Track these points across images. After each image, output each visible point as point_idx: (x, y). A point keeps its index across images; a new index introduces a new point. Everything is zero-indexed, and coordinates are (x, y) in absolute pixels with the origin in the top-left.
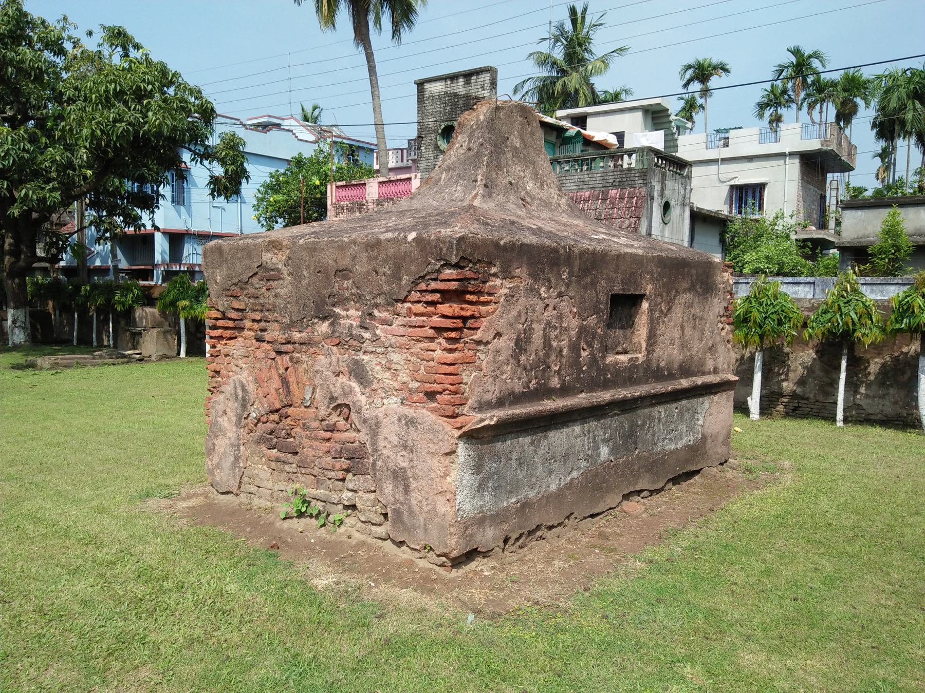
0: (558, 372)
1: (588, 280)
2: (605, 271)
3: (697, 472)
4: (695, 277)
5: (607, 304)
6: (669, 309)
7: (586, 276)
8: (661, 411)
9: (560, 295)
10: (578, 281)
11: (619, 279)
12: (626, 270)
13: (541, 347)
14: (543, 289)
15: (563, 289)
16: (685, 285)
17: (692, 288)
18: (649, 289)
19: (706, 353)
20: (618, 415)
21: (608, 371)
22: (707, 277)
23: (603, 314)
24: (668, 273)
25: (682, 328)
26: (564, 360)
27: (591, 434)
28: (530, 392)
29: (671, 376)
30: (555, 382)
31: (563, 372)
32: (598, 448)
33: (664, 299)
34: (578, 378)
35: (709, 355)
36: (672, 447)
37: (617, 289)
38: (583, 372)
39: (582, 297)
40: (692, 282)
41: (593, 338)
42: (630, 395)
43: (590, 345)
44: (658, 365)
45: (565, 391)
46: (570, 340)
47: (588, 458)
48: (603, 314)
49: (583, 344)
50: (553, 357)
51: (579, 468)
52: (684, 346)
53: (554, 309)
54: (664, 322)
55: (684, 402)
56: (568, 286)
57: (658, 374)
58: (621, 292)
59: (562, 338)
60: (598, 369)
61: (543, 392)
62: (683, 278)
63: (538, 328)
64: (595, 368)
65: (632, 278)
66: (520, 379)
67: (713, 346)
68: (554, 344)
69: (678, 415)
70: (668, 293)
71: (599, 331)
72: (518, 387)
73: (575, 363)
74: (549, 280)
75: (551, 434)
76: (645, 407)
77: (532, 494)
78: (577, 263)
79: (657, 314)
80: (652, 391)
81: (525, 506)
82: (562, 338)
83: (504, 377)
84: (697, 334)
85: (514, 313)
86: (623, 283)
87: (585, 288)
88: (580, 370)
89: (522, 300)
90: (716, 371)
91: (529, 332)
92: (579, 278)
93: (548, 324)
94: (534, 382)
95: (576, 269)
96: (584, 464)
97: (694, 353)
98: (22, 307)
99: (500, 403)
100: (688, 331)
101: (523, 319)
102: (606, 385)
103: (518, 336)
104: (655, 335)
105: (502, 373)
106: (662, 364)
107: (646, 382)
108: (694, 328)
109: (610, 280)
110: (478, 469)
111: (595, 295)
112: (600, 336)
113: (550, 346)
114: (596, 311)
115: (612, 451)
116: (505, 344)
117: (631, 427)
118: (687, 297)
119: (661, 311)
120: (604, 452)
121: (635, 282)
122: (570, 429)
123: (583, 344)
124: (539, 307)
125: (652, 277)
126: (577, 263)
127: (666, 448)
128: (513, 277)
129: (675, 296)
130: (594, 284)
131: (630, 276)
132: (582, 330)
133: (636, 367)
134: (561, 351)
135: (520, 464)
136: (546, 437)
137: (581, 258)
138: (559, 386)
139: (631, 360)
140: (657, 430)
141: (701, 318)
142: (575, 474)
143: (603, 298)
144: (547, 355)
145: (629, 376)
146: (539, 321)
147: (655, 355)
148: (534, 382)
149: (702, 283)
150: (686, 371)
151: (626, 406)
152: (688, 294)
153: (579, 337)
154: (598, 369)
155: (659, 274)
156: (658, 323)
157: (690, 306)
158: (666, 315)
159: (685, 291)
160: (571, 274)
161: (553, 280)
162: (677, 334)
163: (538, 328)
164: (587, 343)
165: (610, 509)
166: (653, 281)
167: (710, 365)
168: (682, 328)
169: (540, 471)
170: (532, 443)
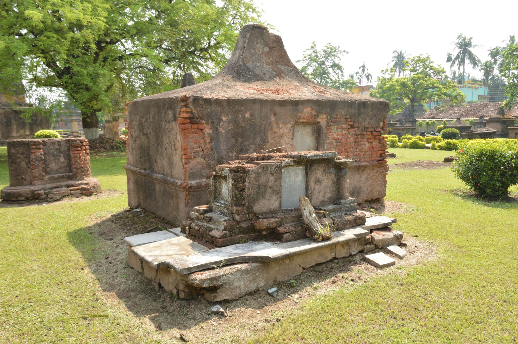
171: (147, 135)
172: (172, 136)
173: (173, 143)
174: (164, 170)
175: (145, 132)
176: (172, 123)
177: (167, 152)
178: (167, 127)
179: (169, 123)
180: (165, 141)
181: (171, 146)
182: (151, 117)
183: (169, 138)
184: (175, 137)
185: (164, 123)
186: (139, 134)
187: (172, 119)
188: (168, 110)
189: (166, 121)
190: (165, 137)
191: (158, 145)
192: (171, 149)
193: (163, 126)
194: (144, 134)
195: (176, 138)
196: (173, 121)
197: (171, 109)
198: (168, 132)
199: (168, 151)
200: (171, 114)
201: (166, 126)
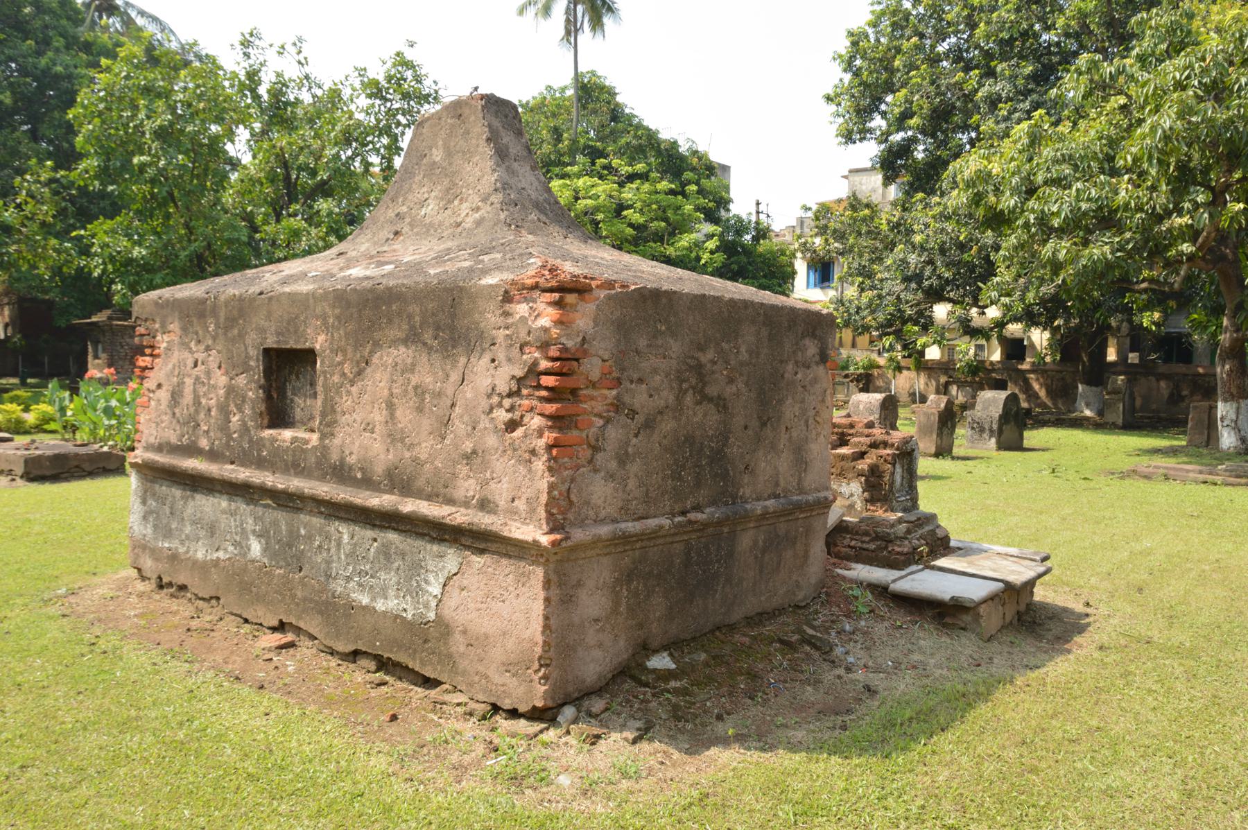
0: (207, 432)
1: (236, 331)
2: (254, 320)
3: (429, 683)
4: (417, 318)
5: (258, 360)
6: (359, 373)
7: (232, 327)
8: (344, 531)
9: (208, 349)
10: (225, 334)
11: (273, 329)
12: (281, 316)
13: (191, 403)
14: (193, 343)
15: (210, 342)
16: (395, 333)
17: (413, 337)
18: (319, 342)
19: (455, 463)
20: (274, 508)
21: (264, 446)
22: (453, 316)
23: (254, 374)
24: (355, 315)
25: (391, 407)
26: (213, 421)
27: (238, 517)
28: (182, 445)
29: (368, 483)
30: (204, 443)
31: (212, 434)
32: (248, 539)
33: (350, 355)
34: (227, 444)
35: (463, 470)
36: (365, 600)
37: (271, 342)
38: (234, 440)
39: (228, 350)
40: (412, 328)
41: (244, 401)
42: (270, 484)
43: (240, 410)
44: (342, 460)
45: (213, 455)
46: (218, 400)
47: (236, 544)
48: (254, 374)
49: (233, 408)
50: (202, 416)
51: (226, 550)
52: (395, 437)
53: (203, 364)
54: (349, 393)
55: (392, 536)
56: (214, 338)
57: (341, 473)
58: (275, 346)
59: (211, 396)
60: (251, 441)
61: (191, 450)
62: (390, 321)
63: (189, 382)
64: (246, 438)
65: (292, 324)
66: (175, 431)
67: (474, 452)
68: (204, 401)
69: (378, 551)
70: (358, 345)
71: (250, 393)
72: (174, 440)
73: (224, 427)
74: (197, 333)
75: (198, 497)
76: (311, 512)
77: (182, 550)
78: (222, 315)
79: (336, 379)
80: (306, 491)
81: (174, 557)
82: (211, 396)
83: (163, 425)
84: (426, 423)
85: (170, 366)
86: (278, 334)
87: (233, 340)
88: (229, 437)
89: (176, 353)
90: (485, 505)
91: (181, 384)
92: (227, 329)
93: (197, 379)
94: (186, 437)
95: (222, 320)
96: (231, 548)
97: (423, 457)
98: (1233, 399)
99: (159, 448)
100: (405, 415)
101: (176, 373)
102: (260, 464)
103: (174, 389)
104: (333, 411)
105: (162, 422)
106: (352, 460)
107: (322, 478)
108: (420, 409)
109: (262, 331)
110: (144, 502)
111: (243, 349)
112: (251, 399)
113: (200, 403)
114: (246, 369)
115: (265, 550)
116: (164, 395)
117: (290, 532)
118: (402, 354)
119: (344, 375)
120: (256, 548)
121: (296, 332)
122: (216, 501)
123: (233, 408)
124: (190, 363)
125: (325, 323)
126: (222, 315)
127: (353, 595)
128: (169, 332)
129: (372, 352)
130: (241, 336)
131: (288, 323)
132: (230, 390)
133: (304, 451)
134: (209, 410)
135: (171, 513)
136: (193, 498)
137: (226, 306)
138: (207, 448)
139: (295, 440)
140: (335, 558)
141: (439, 394)
142: (221, 554)
143: (253, 352)
144: (197, 412)
145: (294, 463)
146: (189, 376)
147: (337, 441)
148: (186, 437)
149: (438, 328)
150: (400, 482)
151: (288, 501)
152: (403, 349)
153: (227, 397)
154: (251, 441)
155: (338, 318)
156: (338, 393)
157: (412, 369)
158: (352, 383)
159: (394, 343)
160: (217, 326)
161: (200, 332)
162: (379, 416)
163: (189, 382)
164: (236, 405)
165: (261, 624)
166: (326, 327)
167: (467, 486)
168: (391, 407)
169: (188, 529)
170: (182, 498)
171: (721, 404)
172: (811, 398)
173: (812, 413)
174: (777, 484)
175: (712, 391)
176: (815, 367)
177: (791, 437)
178: (799, 376)
179: (808, 367)
180: (790, 410)
181: (807, 421)
182: (743, 349)
183: (803, 401)
184: (820, 398)
185: (790, 367)
186: (679, 399)
187: (814, 360)
188: (803, 337)
189: (797, 362)
190: (790, 401)
191: (764, 424)
192: (805, 428)
193: (786, 375)
194: (704, 398)
195: (823, 401)
196: (817, 364)
197: (814, 336)
198: (800, 389)
199: (794, 434)
200: (812, 349)
201: (796, 373)
